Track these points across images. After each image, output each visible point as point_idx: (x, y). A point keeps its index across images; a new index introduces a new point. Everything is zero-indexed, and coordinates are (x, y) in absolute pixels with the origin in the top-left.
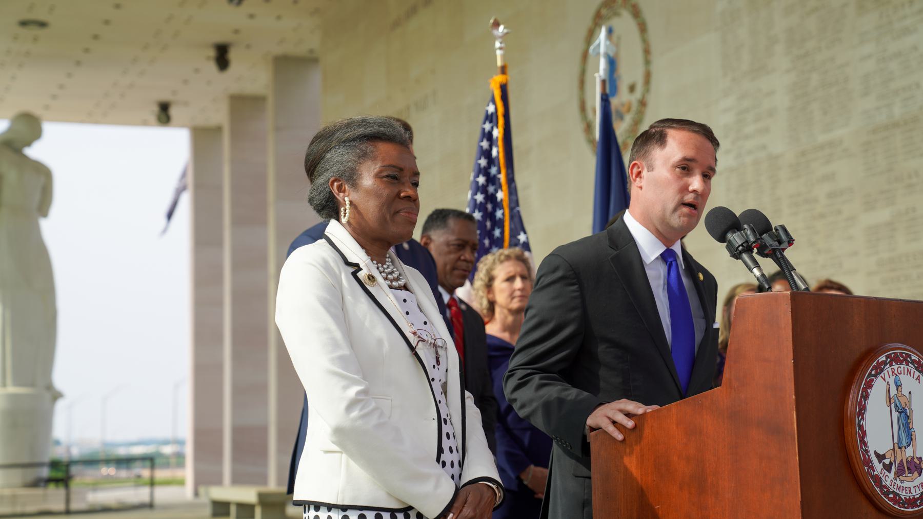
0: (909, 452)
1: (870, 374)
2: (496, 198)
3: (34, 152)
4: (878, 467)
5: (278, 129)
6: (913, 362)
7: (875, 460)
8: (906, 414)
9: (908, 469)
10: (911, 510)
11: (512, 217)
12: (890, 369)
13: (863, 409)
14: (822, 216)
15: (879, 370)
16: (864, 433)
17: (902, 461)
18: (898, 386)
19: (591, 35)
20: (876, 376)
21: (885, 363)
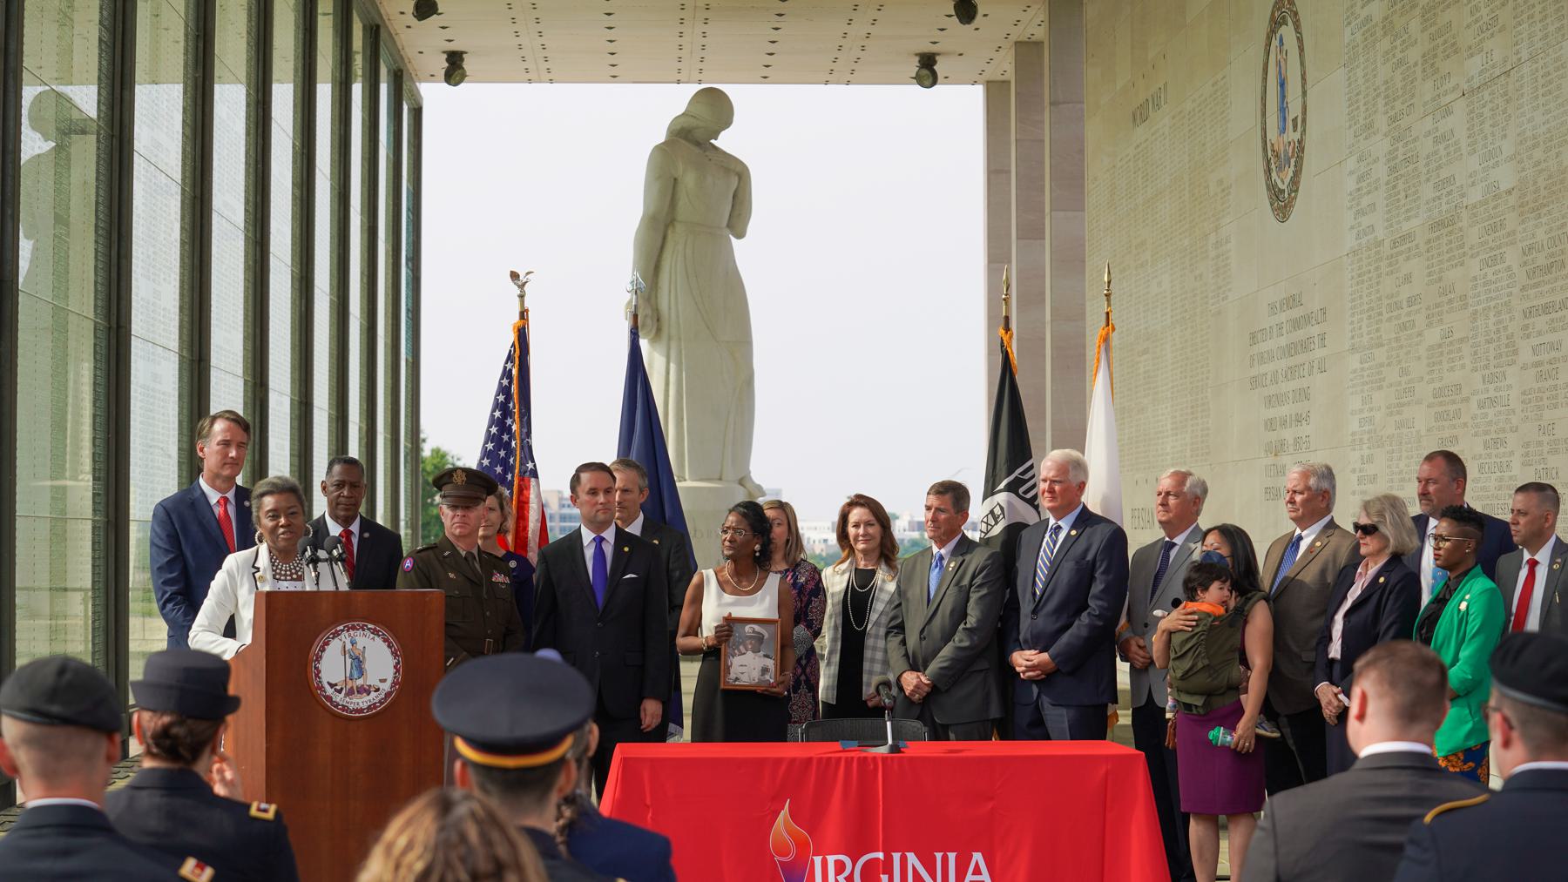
0: (360, 682)
1: (328, 637)
2: (512, 429)
3: (724, 141)
4: (330, 691)
5: (1051, 104)
6: (369, 629)
7: (327, 687)
8: (359, 659)
9: (358, 692)
10: (357, 715)
11: (522, 448)
12: (347, 637)
13: (319, 658)
14: (1403, 327)
15: (336, 634)
16: (319, 672)
17: (352, 688)
18: (353, 643)
19: (1269, 44)
20: (333, 638)
21: (342, 631)
